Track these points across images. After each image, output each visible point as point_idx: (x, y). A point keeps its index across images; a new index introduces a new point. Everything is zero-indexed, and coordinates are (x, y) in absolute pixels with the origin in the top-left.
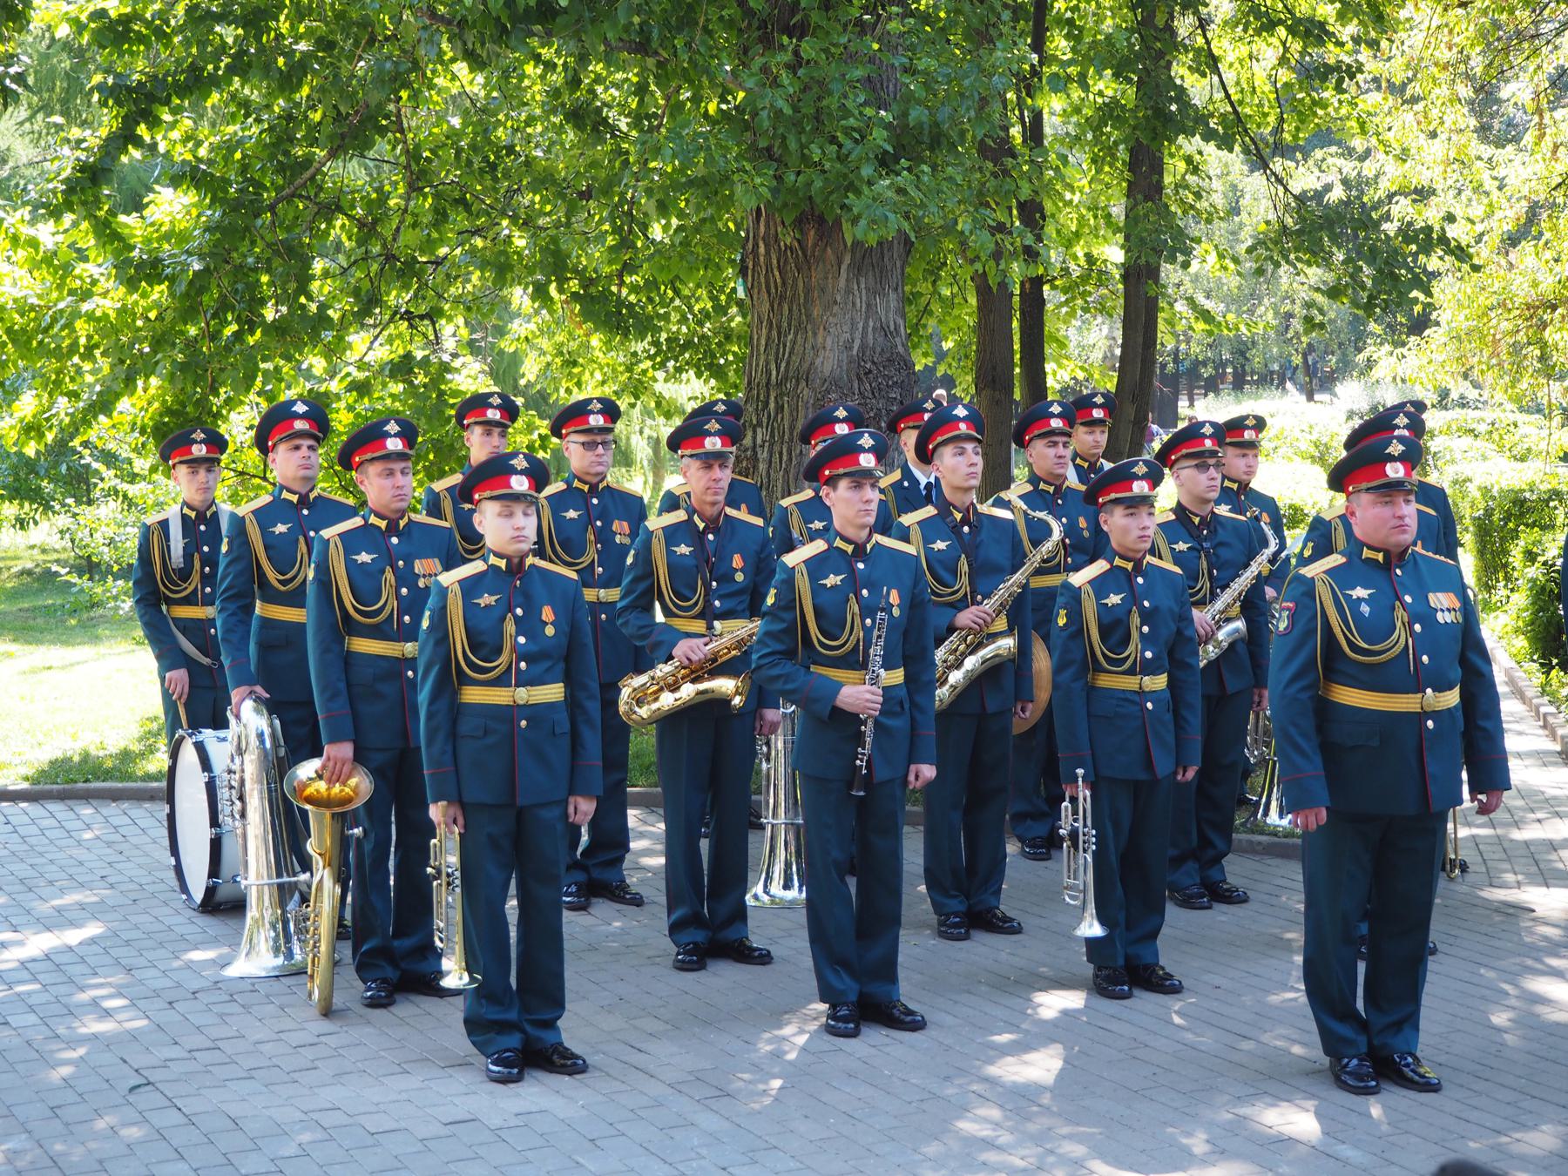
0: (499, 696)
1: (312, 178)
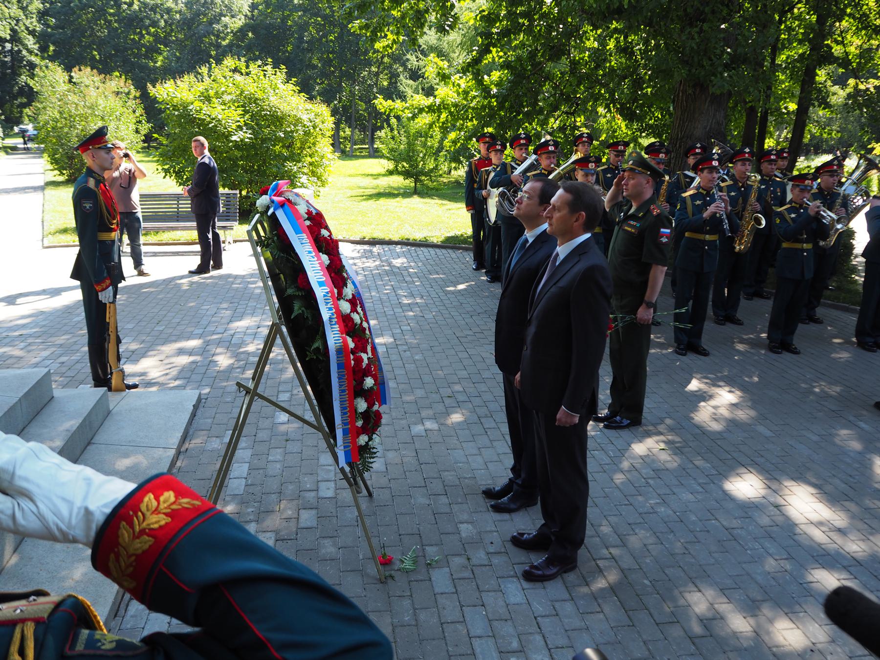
1: (541, 68)
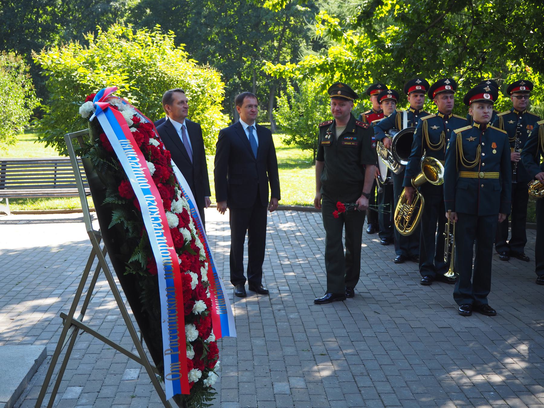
0: (474, 175)
